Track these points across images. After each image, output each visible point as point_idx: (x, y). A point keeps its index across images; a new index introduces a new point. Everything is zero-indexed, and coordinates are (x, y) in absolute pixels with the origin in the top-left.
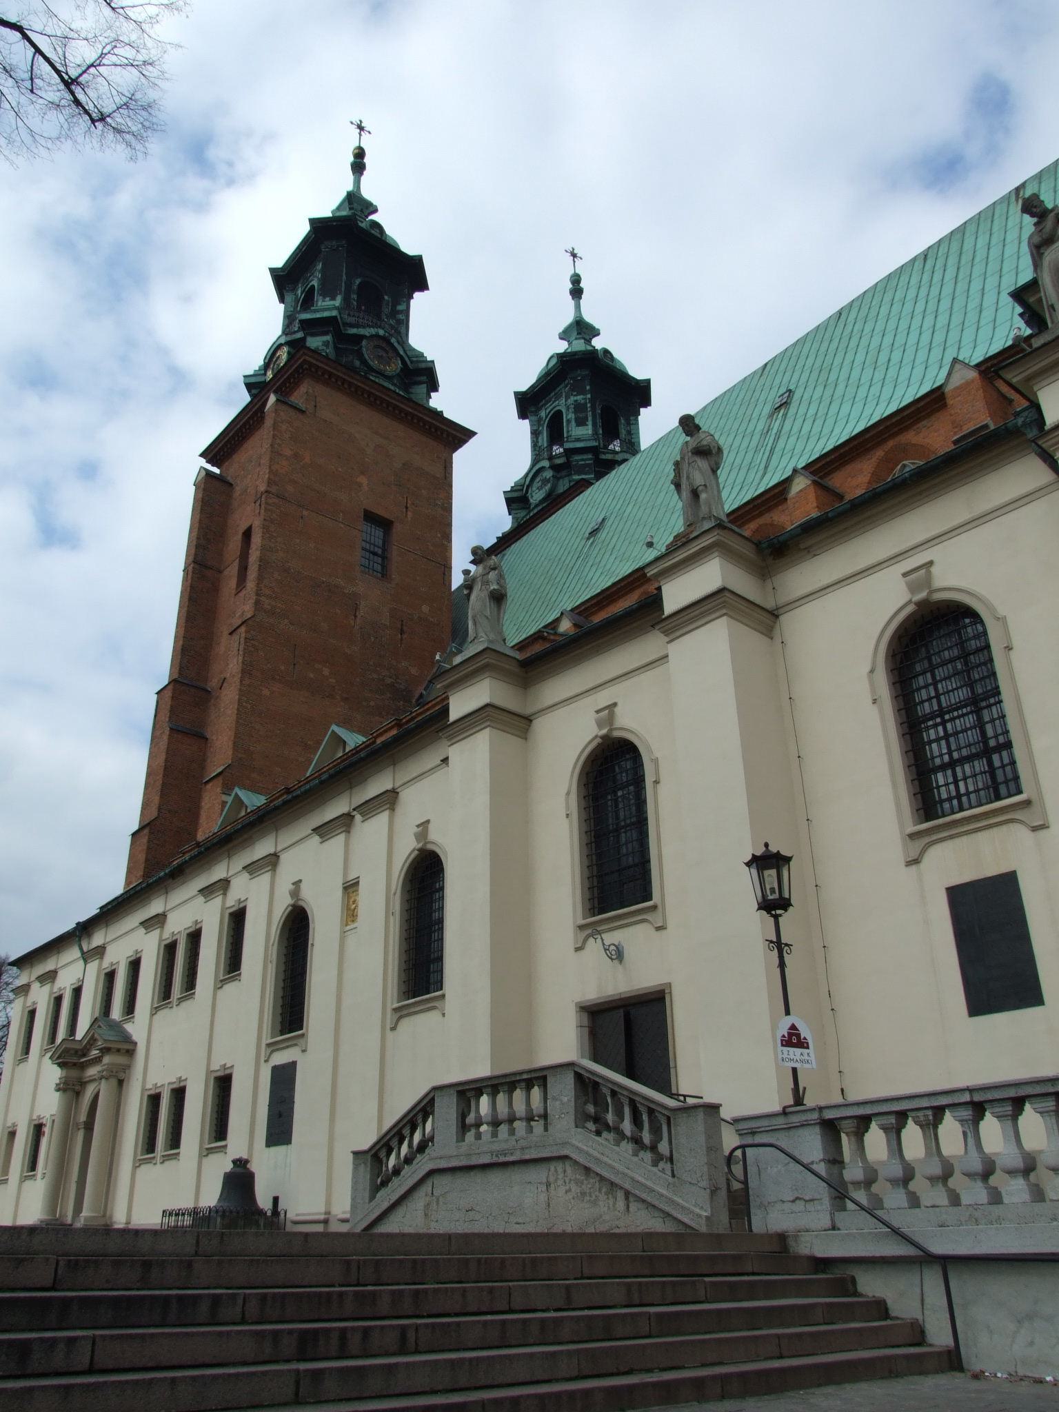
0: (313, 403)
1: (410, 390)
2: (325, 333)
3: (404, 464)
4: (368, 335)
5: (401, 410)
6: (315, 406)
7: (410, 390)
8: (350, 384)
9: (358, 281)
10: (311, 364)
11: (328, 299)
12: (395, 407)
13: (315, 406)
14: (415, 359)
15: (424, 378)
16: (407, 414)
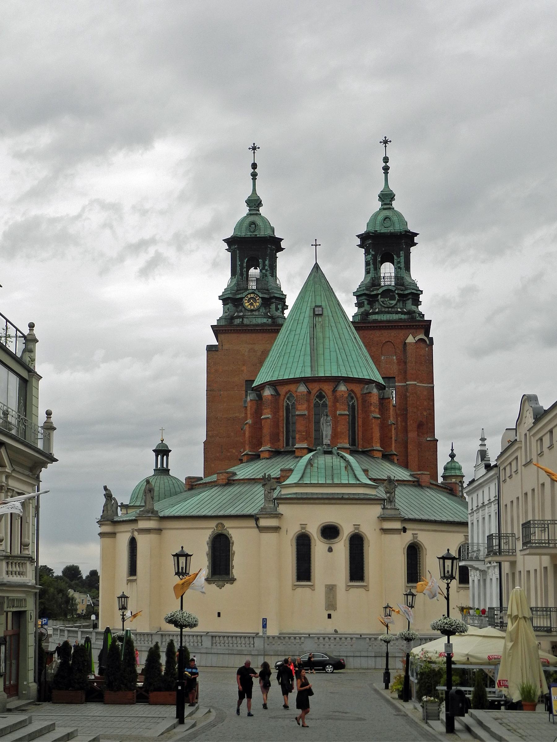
0: (221, 344)
1: (271, 307)
2: (228, 304)
3: (262, 352)
4: (244, 296)
5: (257, 330)
6: (222, 345)
7: (271, 307)
8: (234, 330)
9: (246, 261)
10: (217, 330)
11: (234, 277)
12: (254, 330)
13: (222, 345)
14: (271, 291)
15: (274, 300)
16: (260, 330)
